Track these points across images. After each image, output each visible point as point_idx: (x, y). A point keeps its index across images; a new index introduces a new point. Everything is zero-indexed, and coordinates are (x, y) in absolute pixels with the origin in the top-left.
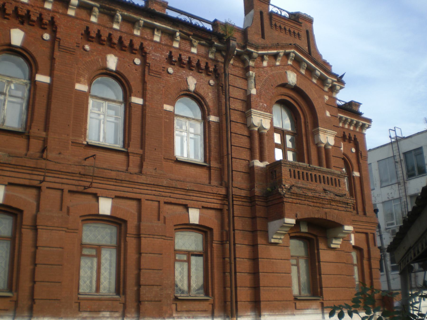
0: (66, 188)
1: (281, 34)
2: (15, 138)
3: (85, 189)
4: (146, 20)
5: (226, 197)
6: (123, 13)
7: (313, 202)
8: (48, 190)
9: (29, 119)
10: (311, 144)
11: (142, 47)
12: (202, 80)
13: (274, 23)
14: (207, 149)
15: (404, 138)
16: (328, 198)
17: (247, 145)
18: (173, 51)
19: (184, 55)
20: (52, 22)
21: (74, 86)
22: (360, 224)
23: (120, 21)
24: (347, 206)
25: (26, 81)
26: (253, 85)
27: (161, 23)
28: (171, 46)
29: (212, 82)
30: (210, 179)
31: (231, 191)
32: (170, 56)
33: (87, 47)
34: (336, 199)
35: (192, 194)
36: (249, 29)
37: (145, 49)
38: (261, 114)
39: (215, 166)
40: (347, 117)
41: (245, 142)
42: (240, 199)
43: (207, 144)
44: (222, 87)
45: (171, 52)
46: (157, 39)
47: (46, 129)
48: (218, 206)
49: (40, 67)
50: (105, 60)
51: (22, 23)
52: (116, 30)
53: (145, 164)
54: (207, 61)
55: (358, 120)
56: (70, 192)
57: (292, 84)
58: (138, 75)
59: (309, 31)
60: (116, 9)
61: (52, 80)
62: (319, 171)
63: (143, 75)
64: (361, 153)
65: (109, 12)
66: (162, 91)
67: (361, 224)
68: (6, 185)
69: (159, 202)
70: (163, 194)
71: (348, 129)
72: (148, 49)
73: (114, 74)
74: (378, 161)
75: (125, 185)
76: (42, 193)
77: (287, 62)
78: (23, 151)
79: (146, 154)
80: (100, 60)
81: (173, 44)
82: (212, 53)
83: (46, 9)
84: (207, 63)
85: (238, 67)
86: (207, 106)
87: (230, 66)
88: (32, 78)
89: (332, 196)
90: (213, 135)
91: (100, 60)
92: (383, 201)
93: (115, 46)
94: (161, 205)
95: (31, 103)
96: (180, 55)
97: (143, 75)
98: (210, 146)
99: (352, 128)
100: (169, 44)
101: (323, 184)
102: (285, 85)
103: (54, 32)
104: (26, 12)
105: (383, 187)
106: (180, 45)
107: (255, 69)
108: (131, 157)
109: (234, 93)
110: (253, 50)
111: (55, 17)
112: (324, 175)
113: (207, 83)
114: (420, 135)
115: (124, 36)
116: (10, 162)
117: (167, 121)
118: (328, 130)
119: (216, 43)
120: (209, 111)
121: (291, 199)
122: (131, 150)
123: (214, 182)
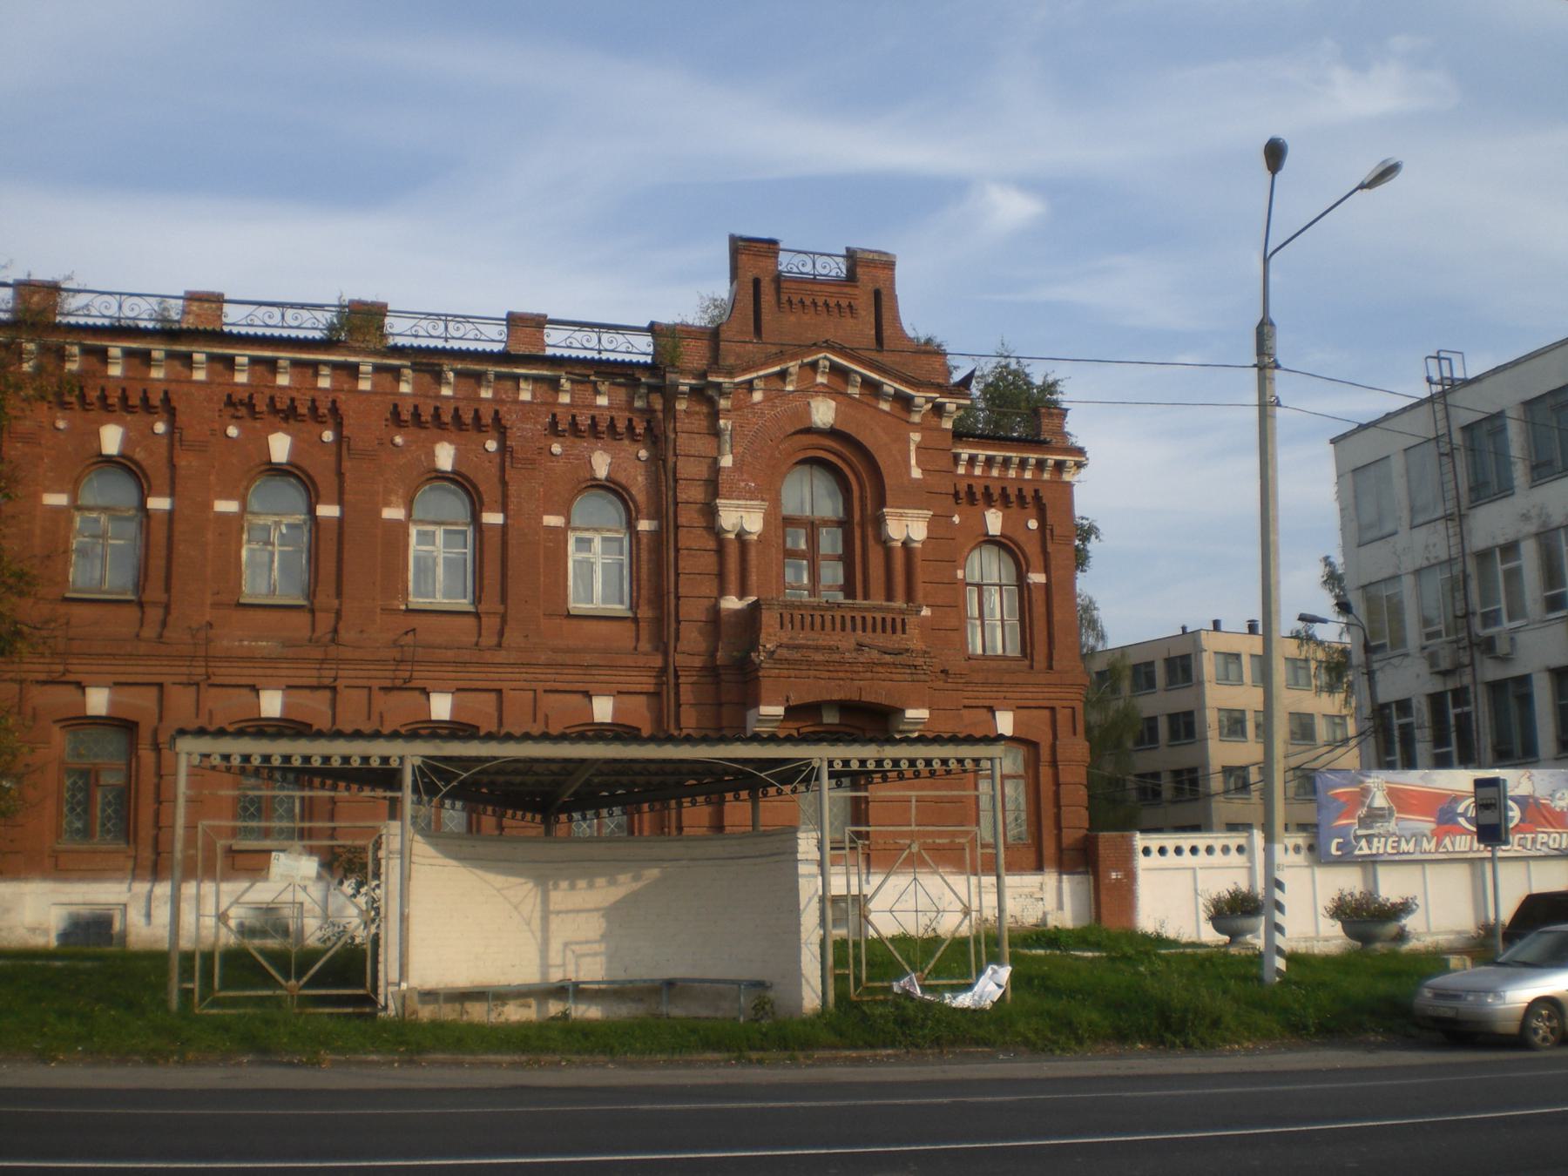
0: (375, 684)
1: (806, 318)
3: (405, 683)
4: (498, 369)
5: (663, 671)
6: (454, 367)
7: (829, 671)
8: (348, 690)
9: (312, 581)
10: (871, 542)
11: (497, 417)
12: (623, 454)
13: (784, 298)
14: (634, 583)
15: (1467, 383)
16: (862, 660)
17: (714, 569)
18: (558, 410)
19: (582, 414)
20: (334, 409)
21: (379, 513)
22: (1031, 690)
23: (452, 380)
24: (914, 671)
25: (303, 517)
26: (728, 447)
27: (527, 368)
28: (555, 404)
29: (643, 454)
30: (638, 640)
31: (671, 660)
32: (554, 423)
33: (398, 440)
34: (883, 661)
35: (596, 672)
36: (724, 328)
37: (503, 422)
38: (739, 506)
39: (646, 616)
40: (1008, 454)
41: (708, 562)
42: (694, 673)
43: (634, 574)
44: (663, 460)
45: (554, 416)
46: (525, 396)
47: (339, 594)
48: (651, 689)
49: (322, 491)
50: (431, 455)
51: (286, 419)
52: (447, 398)
53: (507, 630)
54: (631, 415)
55: (1040, 456)
56: (382, 689)
57: (822, 426)
58: (494, 471)
59: (884, 292)
60: (441, 362)
61: (342, 511)
62: (853, 609)
63: (503, 470)
64: (1052, 530)
65: (430, 368)
66: (539, 491)
67: (1034, 690)
69: (535, 691)
70: (543, 677)
71: (1019, 479)
72: (509, 419)
73: (451, 476)
74: (1405, 450)
75: (472, 669)
76: (338, 697)
77: (815, 379)
78: (307, 633)
79: (509, 611)
80: (423, 457)
81: (557, 399)
82: (640, 397)
83: (320, 389)
84: (630, 420)
85: (697, 413)
86: (634, 502)
87: (680, 416)
88: (311, 511)
89: (875, 654)
90: (644, 556)
91: (423, 457)
92: (1417, 566)
93: (449, 427)
94: (538, 695)
96: (574, 417)
97: (503, 470)
98: (638, 580)
99: (1028, 475)
100: (551, 400)
101: (859, 632)
102: (810, 430)
104: (289, 402)
105: (1415, 527)
106: (572, 397)
107: (732, 414)
108: (484, 620)
109: (691, 468)
110: (721, 380)
112: (865, 614)
113: (634, 457)
114: (1500, 377)
115: (461, 405)
117: (551, 545)
118: (906, 511)
119: (643, 380)
120: (638, 511)
121: (777, 671)
122: (483, 608)
123: (645, 645)
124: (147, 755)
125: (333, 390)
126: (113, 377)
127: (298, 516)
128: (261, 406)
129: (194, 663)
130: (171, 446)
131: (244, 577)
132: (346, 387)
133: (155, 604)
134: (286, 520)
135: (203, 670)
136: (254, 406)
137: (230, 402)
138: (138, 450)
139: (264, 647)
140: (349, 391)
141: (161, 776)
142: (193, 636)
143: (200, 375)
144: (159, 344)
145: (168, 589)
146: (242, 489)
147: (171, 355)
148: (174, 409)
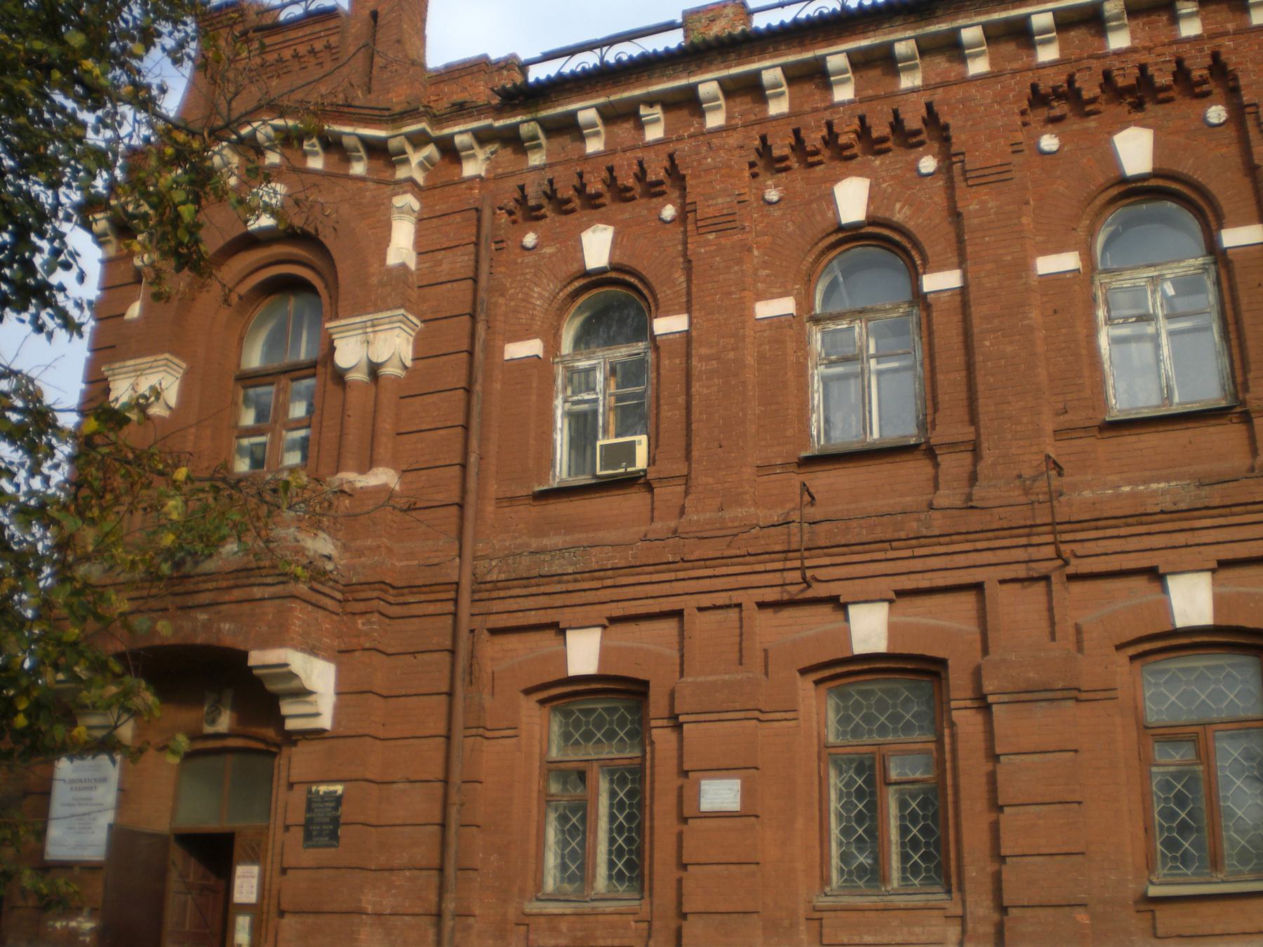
2: (1211, 429)
9: (1237, 364)
20: (1218, 68)
25: (1200, 261)
49: (1226, 207)
51: (1138, 106)
68: (1213, 571)
83: (1188, 40)
88: (1213, 248)
95: (1230, 320)
103: (1232, 94)
111: (1223, 50)
116: (1206, 502)
124: (967, 720)
125: (1208, 36)
126: (842, 104)
127: (1192, 261)
128: (1089, 87)
129: (1035, 540)
130: (950, 187)
131: (1110, 381)
132: (1230, 27)
133: (952, 446)
134: (1169, 273)
135: (1049, 551)
136: (1079, 91)
137: (1038, 98)
138: (898, 206)
139: (1164, 492)
140: (1238, 32)
141: (995, 758)
142: (1026, 492)
143: (979, 66)
144: (905, 30)
145: (973, 420)
146: (1081, 233)
147: (927, 48)
148: (946, 127)
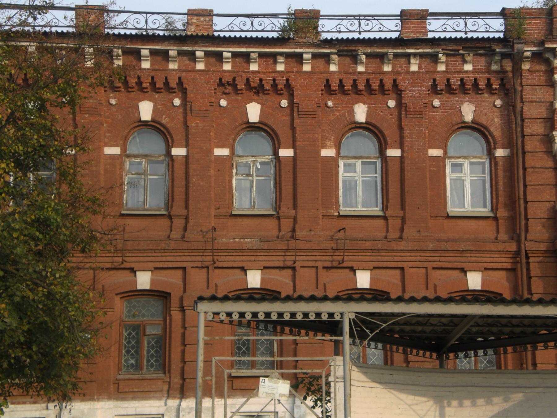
0: (320, 265)
2: (266, 220)
3: (340, 263)
4: (395, 51)
5: (517, 253)
6: (366, 51)
8: (303, 269)
9: (278, 198)
11: (395, 84)
12: (483, 104)
14: (494, 193)
18: (437, 76)
20: (288, 85)
23: (364, 60)
25: (270, 157)
27: (416, 49)
29: (498, 103)
30: (498, 232)
33: (330, 103)
39: (504, 215)
42: (540, 255)
43: (494, 187)
44: (513, 106)
45: (434, 80)
46: (414, 68)
47: (295, 207)
48: (509, 266)
50: (352, 112)
51: (257, 93)
52: (361, 73)
53: (406, 227)
56: (324, 268)
58: (394, 120)
60: (357, 48)
61: (295, 153)
63: (400, 119)
65: (349, 53)
66: (425, 133)
69: (426, 268)
72: (403, 85)
73: (365, 126)
76: (296, 273)
78: (275, 233)
79: (407, 214)
81: (436, 68)
82: (495, 63)
83: (279, 72)
84: (489, 80)
86: (493, 137)
87: (525, 74)
88: (275, 153)
90: (501, 174)
93: (363, 93)
94: (429, 272)
95: (278, 182)
96: (448, 80)
97: (400, 119)
98: (497, 190)
100: (432, 69)
103: (291, 97)
108: (390, 221)
111: (290, 79)
113: (492, 105)
115: (371, 77)
116: (262, 247)
117: (435, 169)
119: (498, 50)
120: (495, 143)
123: (503, 236)
124: (176, 315)
126: (145, 69)
127: (267, 157)
128: (241, 85)
129: (205, 254)
130: (185, 113)
131: (235, 197)
132: (295, 69)
133: (178, 216)
134: (260, 160)
135: (210, 258)
136: (237, 85)
137: (221, 83)
138: (164, 117)
139: (249, 242)
140: (297, 72)
141: (185, 328)
142: (204, 237)
143: (200, 66)
144: (174, 46)
145: (187, 207)
146: (231, 141)
147: (181, 53)
148: (186, 89)
